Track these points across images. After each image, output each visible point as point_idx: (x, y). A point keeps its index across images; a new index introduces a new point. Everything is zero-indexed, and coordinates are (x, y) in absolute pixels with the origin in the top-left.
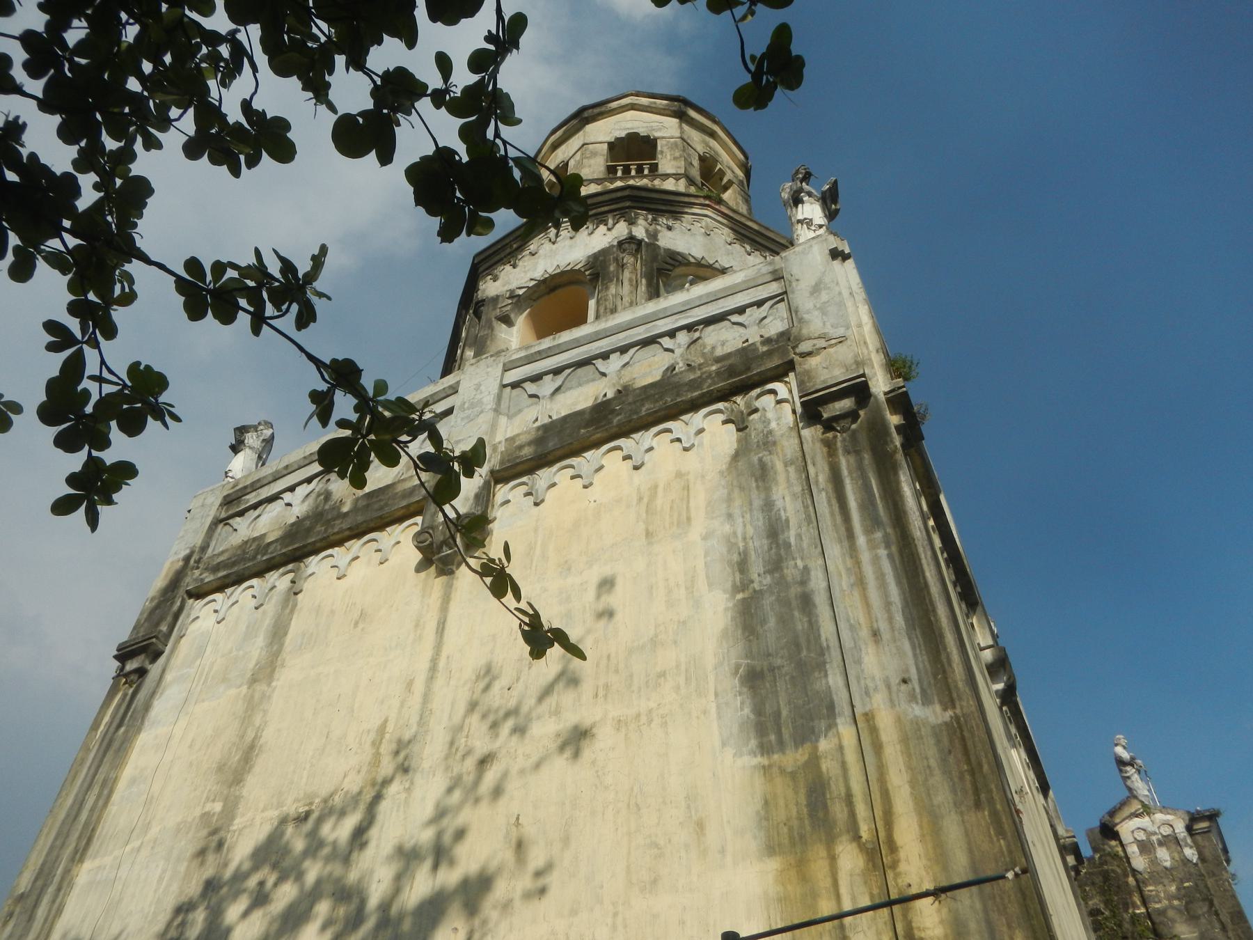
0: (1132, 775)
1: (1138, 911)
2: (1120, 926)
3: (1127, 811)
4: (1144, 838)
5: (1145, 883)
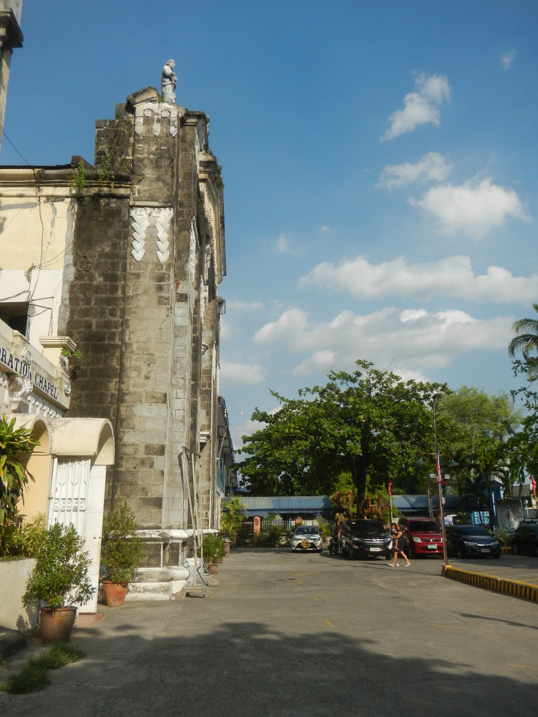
0: (168, 84)
1: (127, 158)
2: (113, 162)
3: (146, 96)
4: (150, 116)
5: (138, 142)
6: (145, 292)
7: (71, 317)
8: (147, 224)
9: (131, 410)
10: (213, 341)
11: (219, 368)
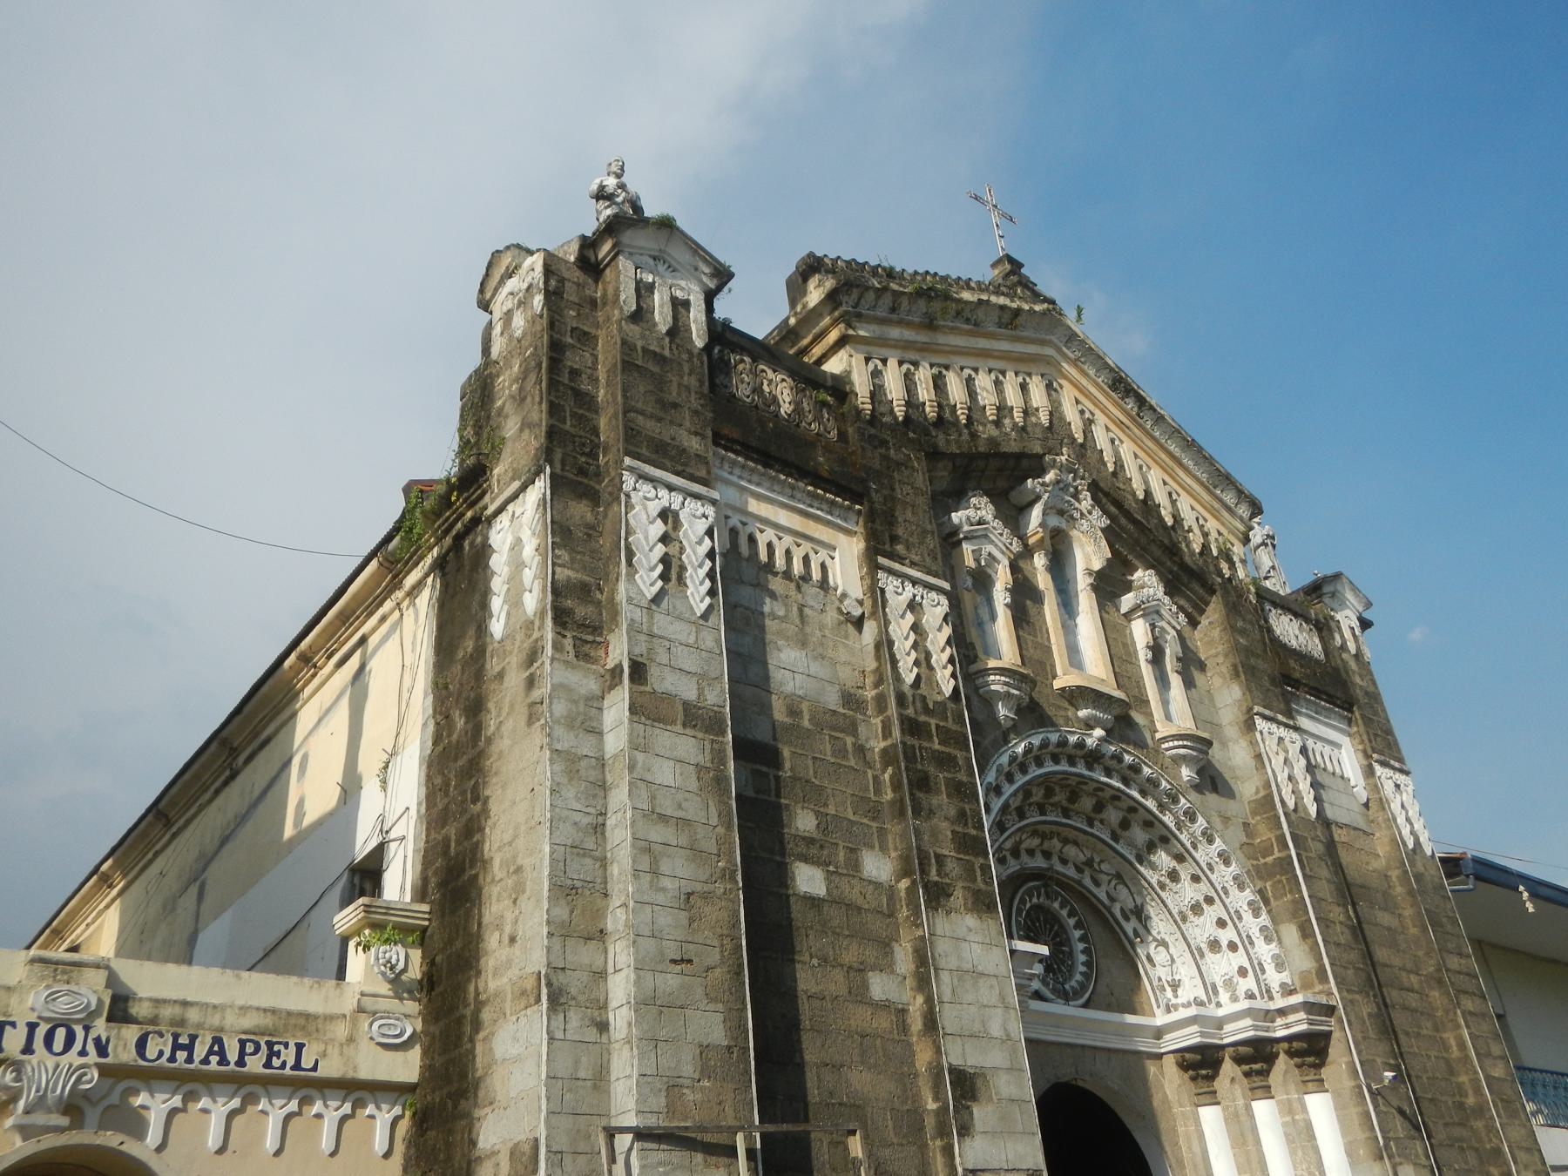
6: (512, 706)
7: (427, 842)
8: (510, 539)
9: (491, 1049)
10: (1252, 709)
11: (1407, 773)
